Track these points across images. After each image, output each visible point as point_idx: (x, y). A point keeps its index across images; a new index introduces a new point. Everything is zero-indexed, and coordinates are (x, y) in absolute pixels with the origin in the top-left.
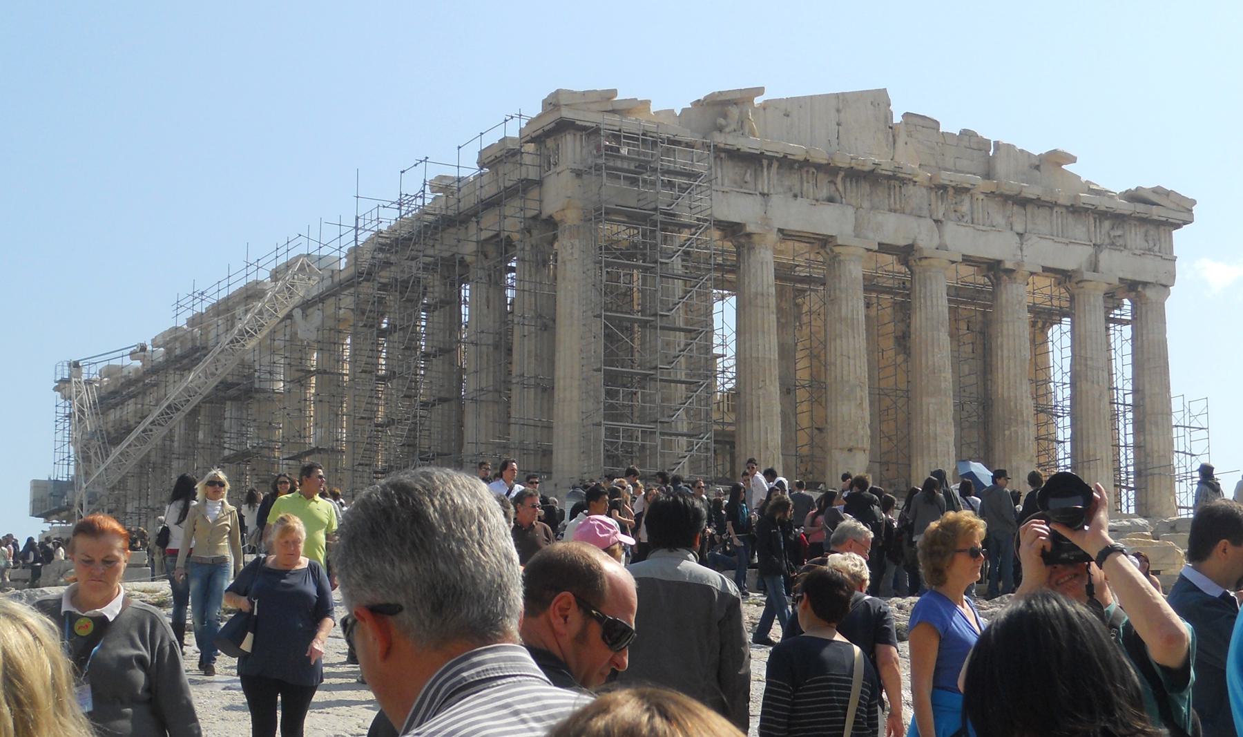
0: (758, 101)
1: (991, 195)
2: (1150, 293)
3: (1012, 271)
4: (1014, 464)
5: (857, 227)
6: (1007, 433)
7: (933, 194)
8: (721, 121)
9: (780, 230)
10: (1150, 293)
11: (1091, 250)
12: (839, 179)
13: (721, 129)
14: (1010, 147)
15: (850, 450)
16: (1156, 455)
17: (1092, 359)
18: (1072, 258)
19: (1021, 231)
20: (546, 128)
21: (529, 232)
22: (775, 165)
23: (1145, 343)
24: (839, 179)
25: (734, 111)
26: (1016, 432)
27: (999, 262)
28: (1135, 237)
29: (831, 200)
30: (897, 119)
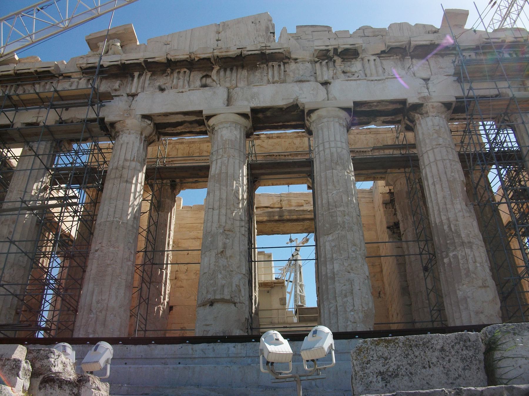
1: (382, 54)
5: (229, 101)
6: (446, 260)
19: (425, 76)
27: (403, 102)
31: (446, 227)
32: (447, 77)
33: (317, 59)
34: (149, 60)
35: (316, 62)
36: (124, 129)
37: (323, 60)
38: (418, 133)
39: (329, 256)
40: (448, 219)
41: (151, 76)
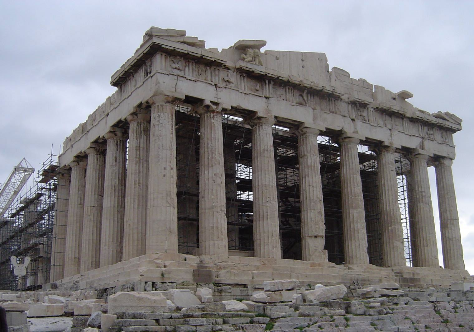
0: (263, 50)
1: (377, 109)
2: (446, 162)
3: (388, 147)
4: (395, 244)
5: (314, 119)
6: (390, 228)
7: (350, 106)
8: (244, 56)
9: (275, 116)
10: (446, 162)
11: (420, 140)
12: (304, 95)
13: (243, 59)
14: (382, 88)
15: (316, 237)
16: (454, 239)
17: (425, 192)
18: (413, 143)
19: (390, 128)
20: (145, 52)
21: (136, 115)
22: (272, 83)
23: (445, 185)
24: (304, 95)
25: (250, 50)
26: (395, 228)
27: (381, 142)
28: (438, 135)
29: (301, 104)
30: (330, 70)
31: (392, 213)
32: (398, 132)
33: (350, 102)
34: (280, 78)
35: (349, 103)
36: (267, 123)
37: (353, 104)
38: (383, 160)
39: (355, 220)
40: (393, 210)
41: (273, 85)
